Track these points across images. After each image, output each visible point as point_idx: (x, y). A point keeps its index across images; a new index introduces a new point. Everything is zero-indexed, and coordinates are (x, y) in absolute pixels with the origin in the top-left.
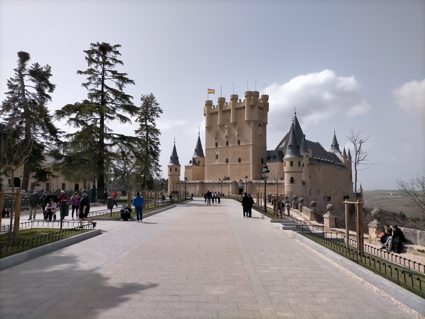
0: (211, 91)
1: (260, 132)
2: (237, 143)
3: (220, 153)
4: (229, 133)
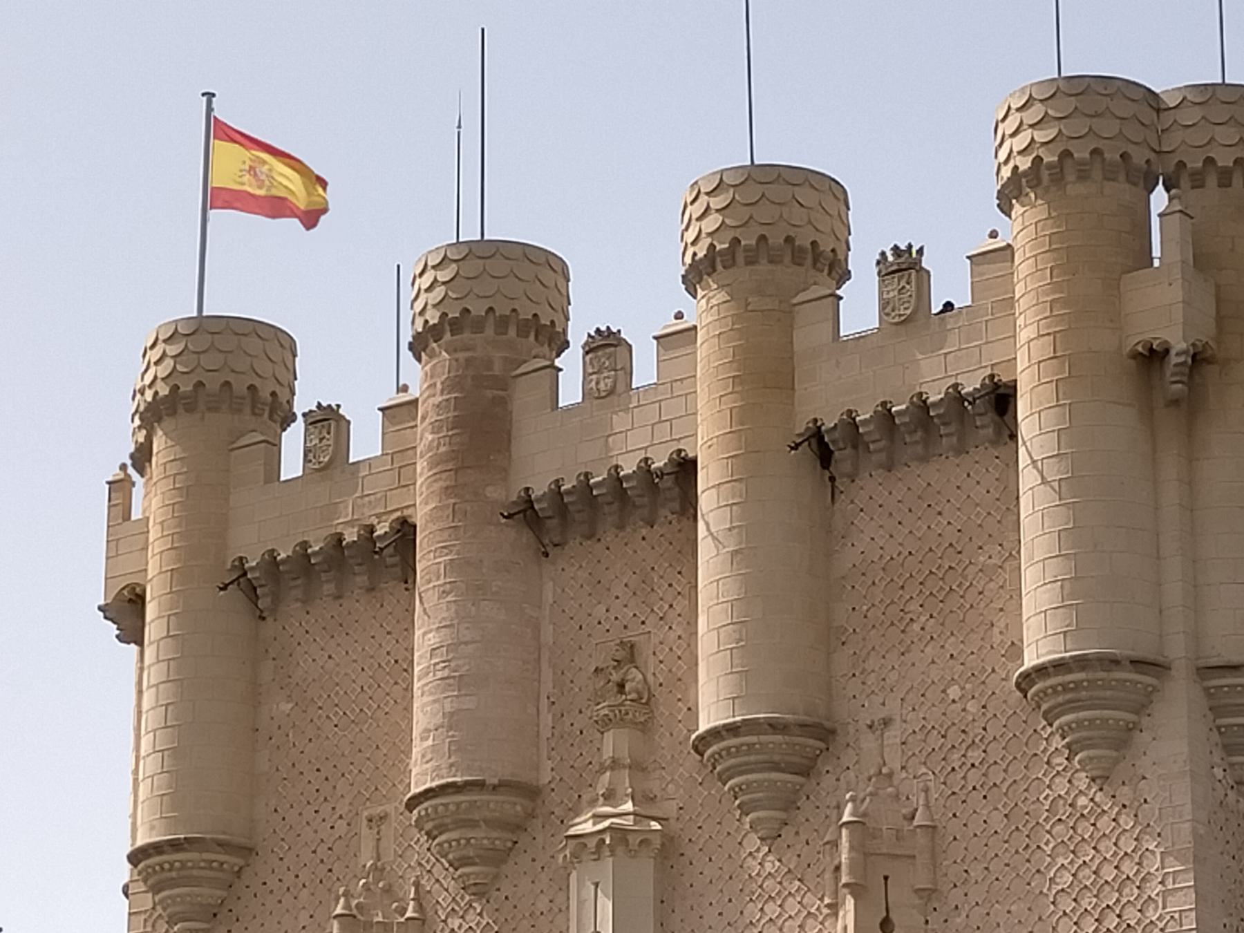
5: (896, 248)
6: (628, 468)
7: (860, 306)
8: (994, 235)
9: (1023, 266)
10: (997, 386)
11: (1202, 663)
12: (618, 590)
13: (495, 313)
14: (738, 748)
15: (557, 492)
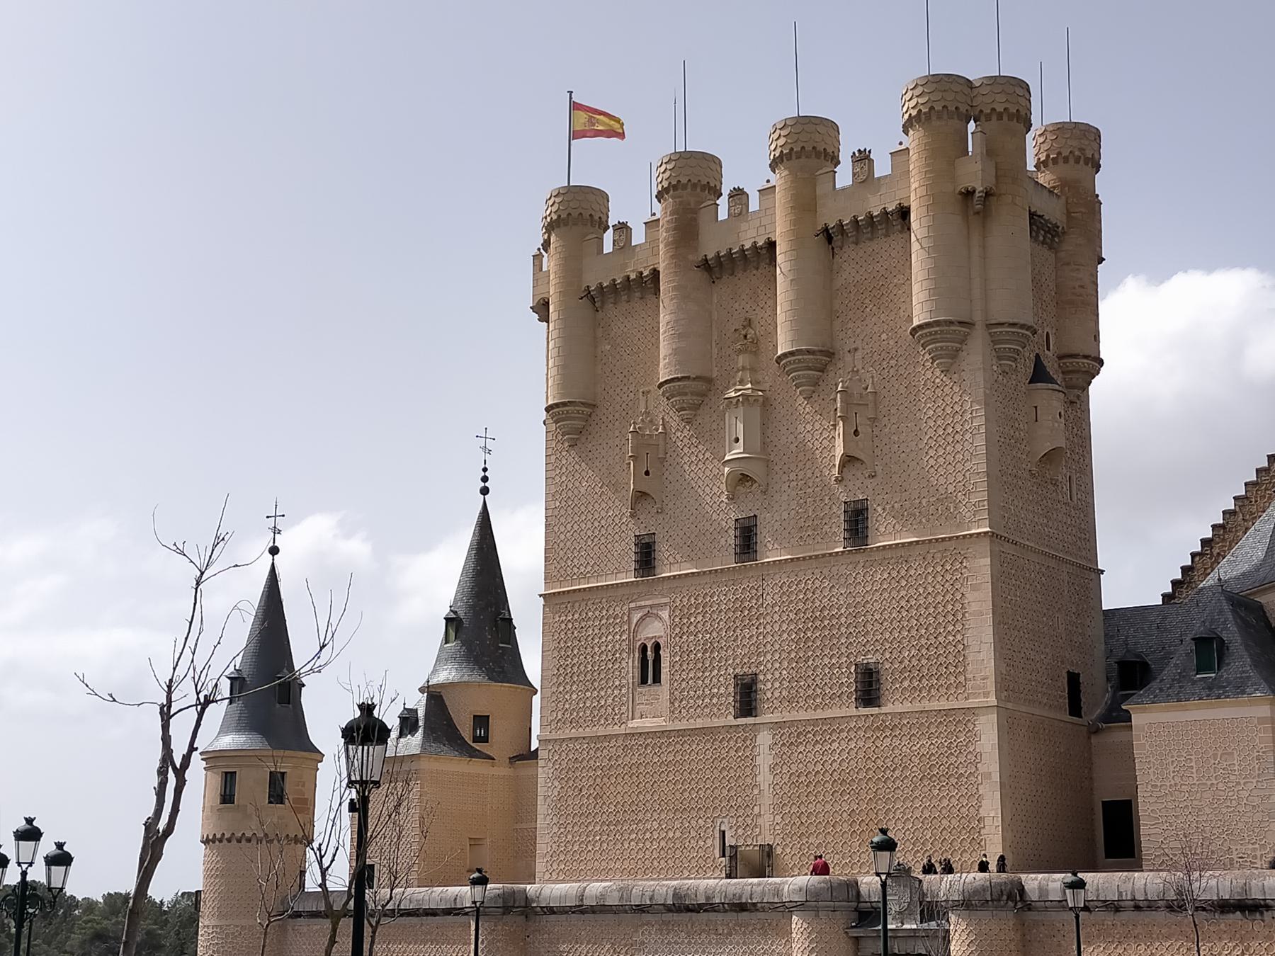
0: (592, 123)
1: (1050, 435)
2: (839, 526)
3: (680, 627)
4: (765, 445)
7: (844, 176)
8: (901, 143)
9: (913, 156)
13: (691, 181)
15: (718, 256)
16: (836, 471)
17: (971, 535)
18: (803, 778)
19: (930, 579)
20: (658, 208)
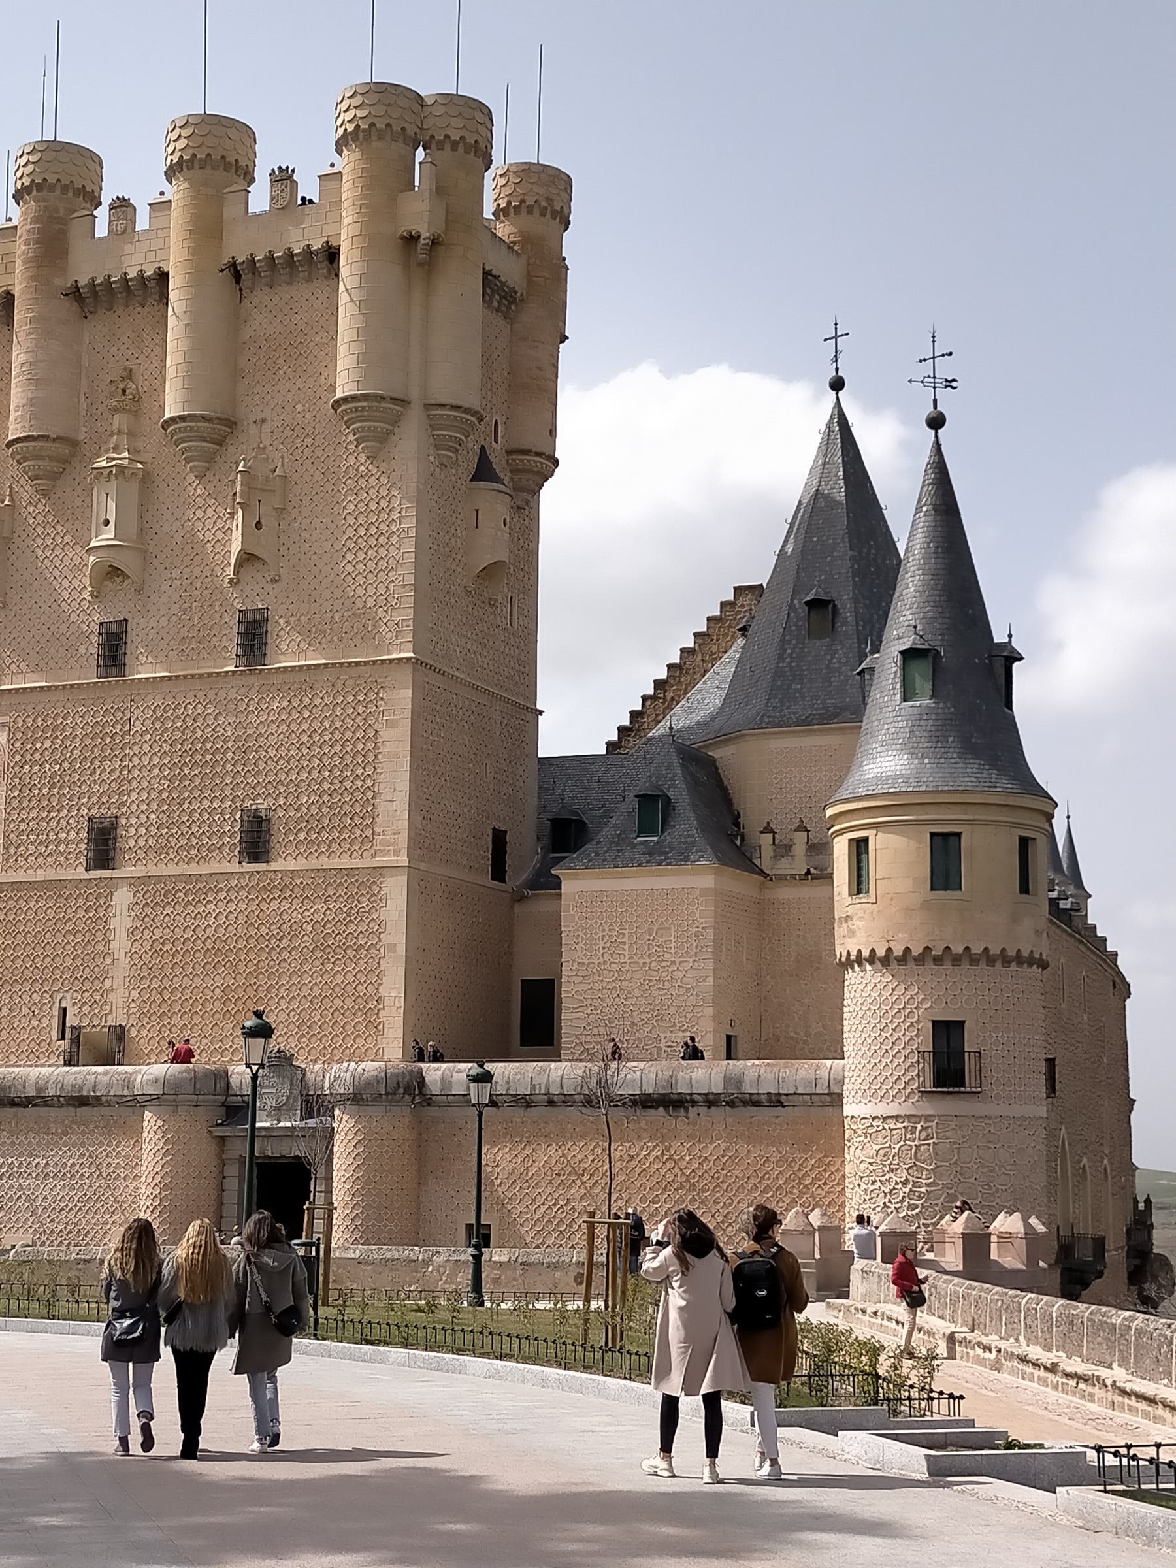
1: (492, 547)
2: (231, 641)
4: (141, 532)
5: (280, 168)
6: (132, 274)
7: (259, 198)
8: (332, 165)
9: (347, 183)
10: (330, 247)
11: (427, 402)
12: (124, 339)
14: (185, 428)
15: (92, 284)
16: (230, 571)
17: (391, 660)
18: (168, 946)
19: (338, 711)
20: (15, 212)
